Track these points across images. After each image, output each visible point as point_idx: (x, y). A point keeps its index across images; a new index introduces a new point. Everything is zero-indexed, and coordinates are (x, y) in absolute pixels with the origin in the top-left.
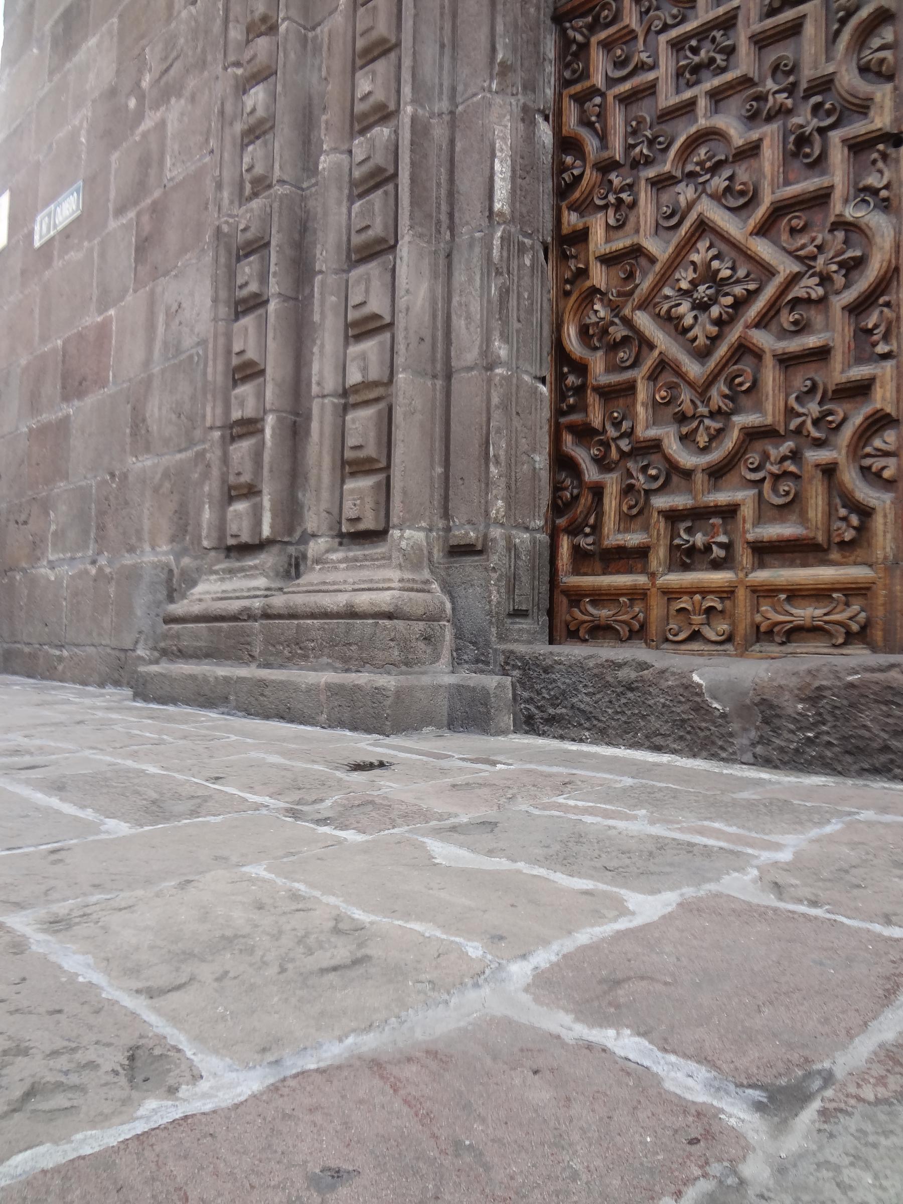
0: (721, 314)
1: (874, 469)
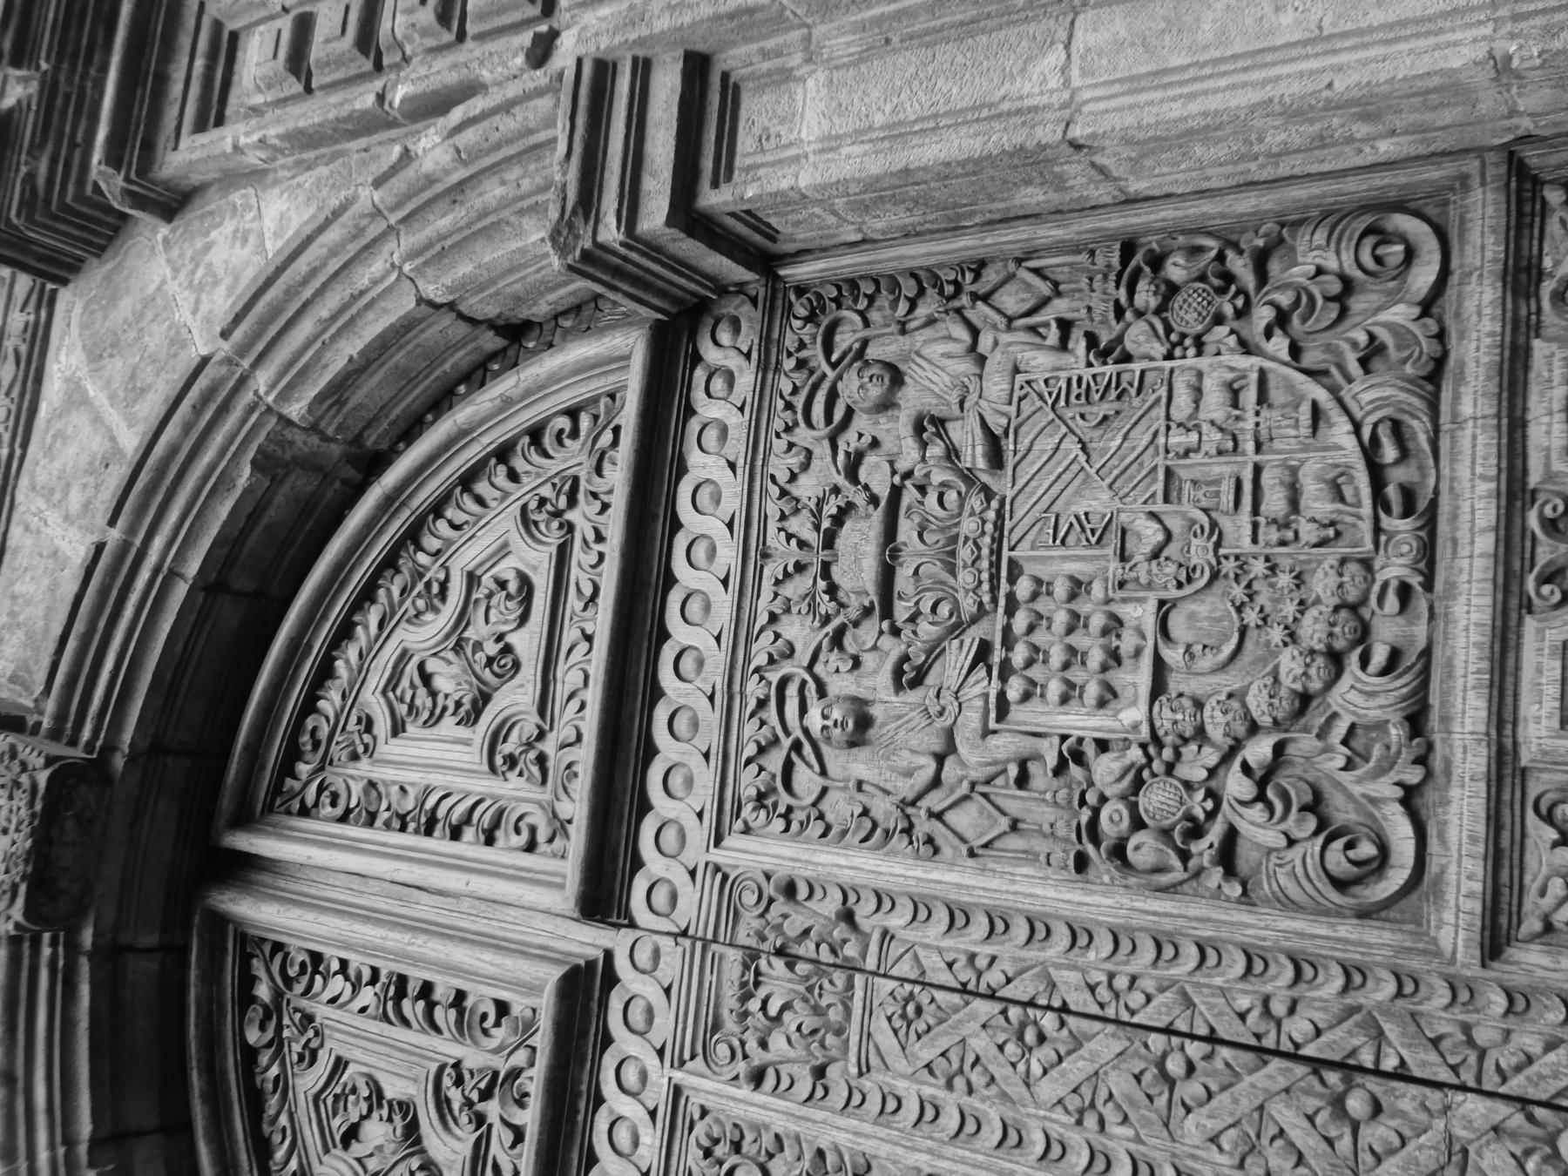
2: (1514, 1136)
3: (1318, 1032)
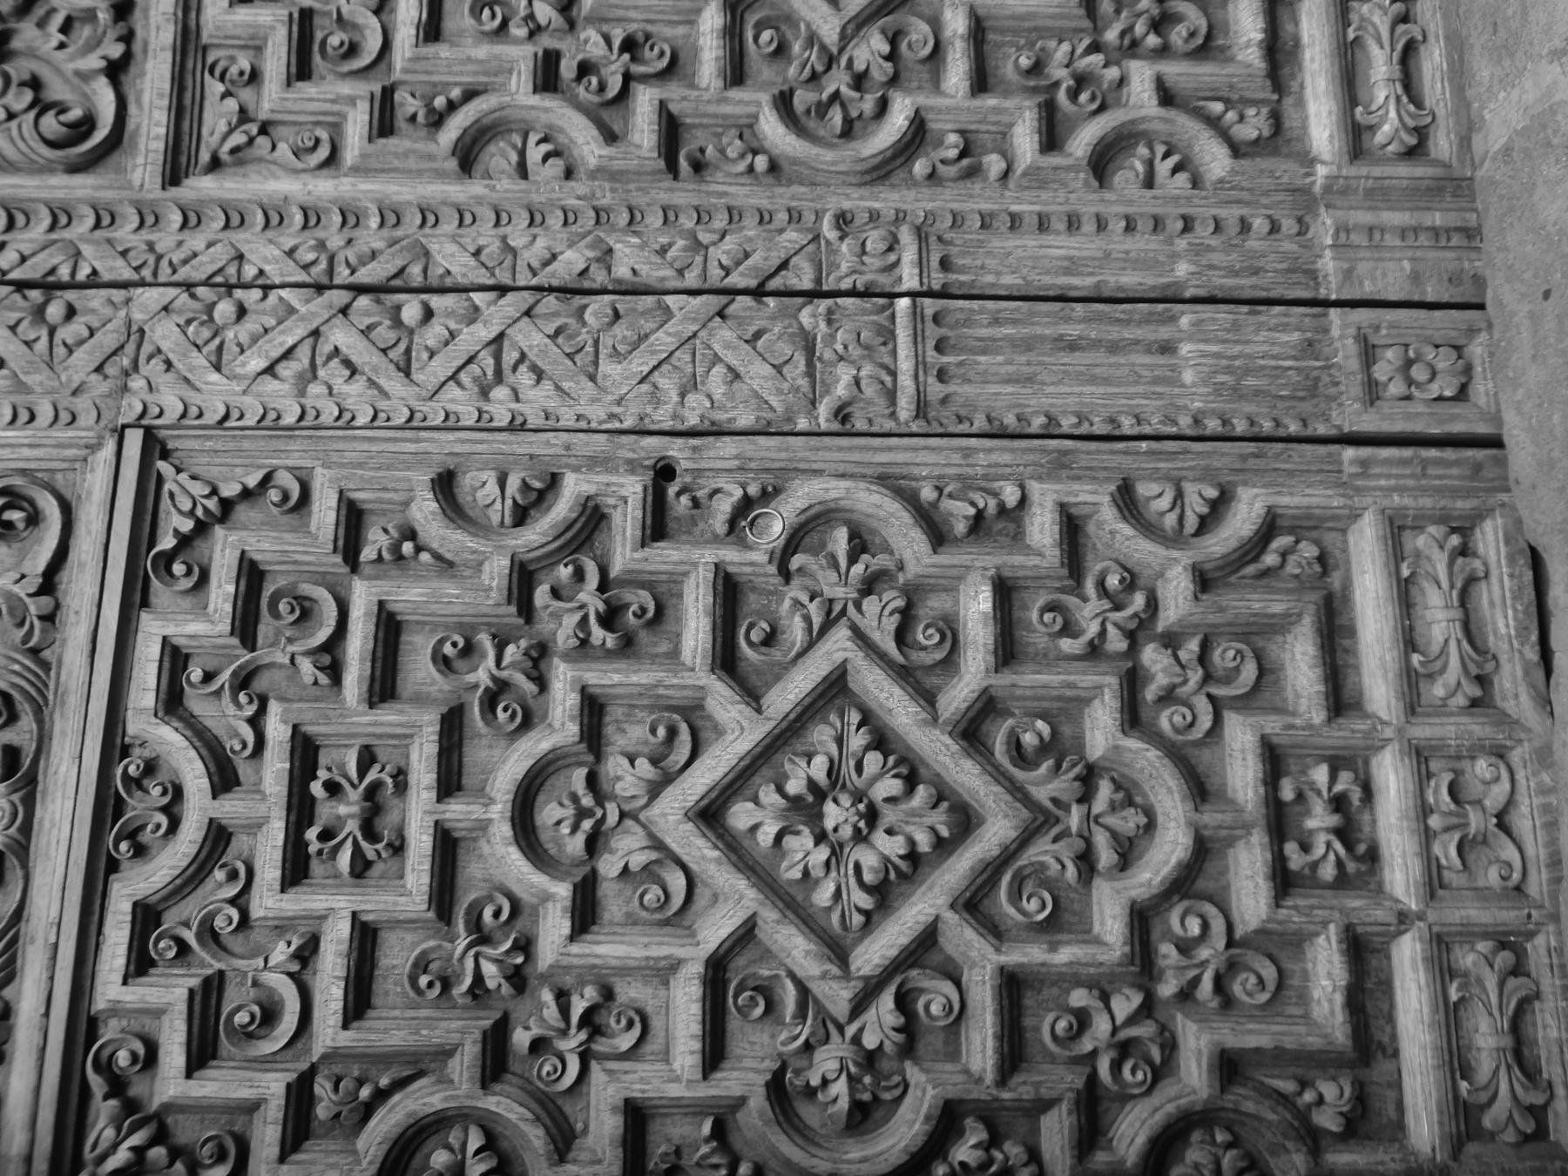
0: (895, 776)
1: (1205, 510)
2: (180, 312)
3: (23, 259)
